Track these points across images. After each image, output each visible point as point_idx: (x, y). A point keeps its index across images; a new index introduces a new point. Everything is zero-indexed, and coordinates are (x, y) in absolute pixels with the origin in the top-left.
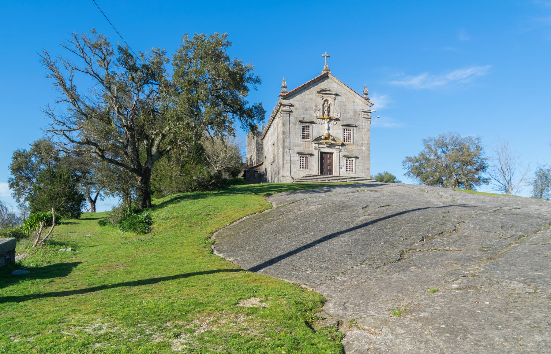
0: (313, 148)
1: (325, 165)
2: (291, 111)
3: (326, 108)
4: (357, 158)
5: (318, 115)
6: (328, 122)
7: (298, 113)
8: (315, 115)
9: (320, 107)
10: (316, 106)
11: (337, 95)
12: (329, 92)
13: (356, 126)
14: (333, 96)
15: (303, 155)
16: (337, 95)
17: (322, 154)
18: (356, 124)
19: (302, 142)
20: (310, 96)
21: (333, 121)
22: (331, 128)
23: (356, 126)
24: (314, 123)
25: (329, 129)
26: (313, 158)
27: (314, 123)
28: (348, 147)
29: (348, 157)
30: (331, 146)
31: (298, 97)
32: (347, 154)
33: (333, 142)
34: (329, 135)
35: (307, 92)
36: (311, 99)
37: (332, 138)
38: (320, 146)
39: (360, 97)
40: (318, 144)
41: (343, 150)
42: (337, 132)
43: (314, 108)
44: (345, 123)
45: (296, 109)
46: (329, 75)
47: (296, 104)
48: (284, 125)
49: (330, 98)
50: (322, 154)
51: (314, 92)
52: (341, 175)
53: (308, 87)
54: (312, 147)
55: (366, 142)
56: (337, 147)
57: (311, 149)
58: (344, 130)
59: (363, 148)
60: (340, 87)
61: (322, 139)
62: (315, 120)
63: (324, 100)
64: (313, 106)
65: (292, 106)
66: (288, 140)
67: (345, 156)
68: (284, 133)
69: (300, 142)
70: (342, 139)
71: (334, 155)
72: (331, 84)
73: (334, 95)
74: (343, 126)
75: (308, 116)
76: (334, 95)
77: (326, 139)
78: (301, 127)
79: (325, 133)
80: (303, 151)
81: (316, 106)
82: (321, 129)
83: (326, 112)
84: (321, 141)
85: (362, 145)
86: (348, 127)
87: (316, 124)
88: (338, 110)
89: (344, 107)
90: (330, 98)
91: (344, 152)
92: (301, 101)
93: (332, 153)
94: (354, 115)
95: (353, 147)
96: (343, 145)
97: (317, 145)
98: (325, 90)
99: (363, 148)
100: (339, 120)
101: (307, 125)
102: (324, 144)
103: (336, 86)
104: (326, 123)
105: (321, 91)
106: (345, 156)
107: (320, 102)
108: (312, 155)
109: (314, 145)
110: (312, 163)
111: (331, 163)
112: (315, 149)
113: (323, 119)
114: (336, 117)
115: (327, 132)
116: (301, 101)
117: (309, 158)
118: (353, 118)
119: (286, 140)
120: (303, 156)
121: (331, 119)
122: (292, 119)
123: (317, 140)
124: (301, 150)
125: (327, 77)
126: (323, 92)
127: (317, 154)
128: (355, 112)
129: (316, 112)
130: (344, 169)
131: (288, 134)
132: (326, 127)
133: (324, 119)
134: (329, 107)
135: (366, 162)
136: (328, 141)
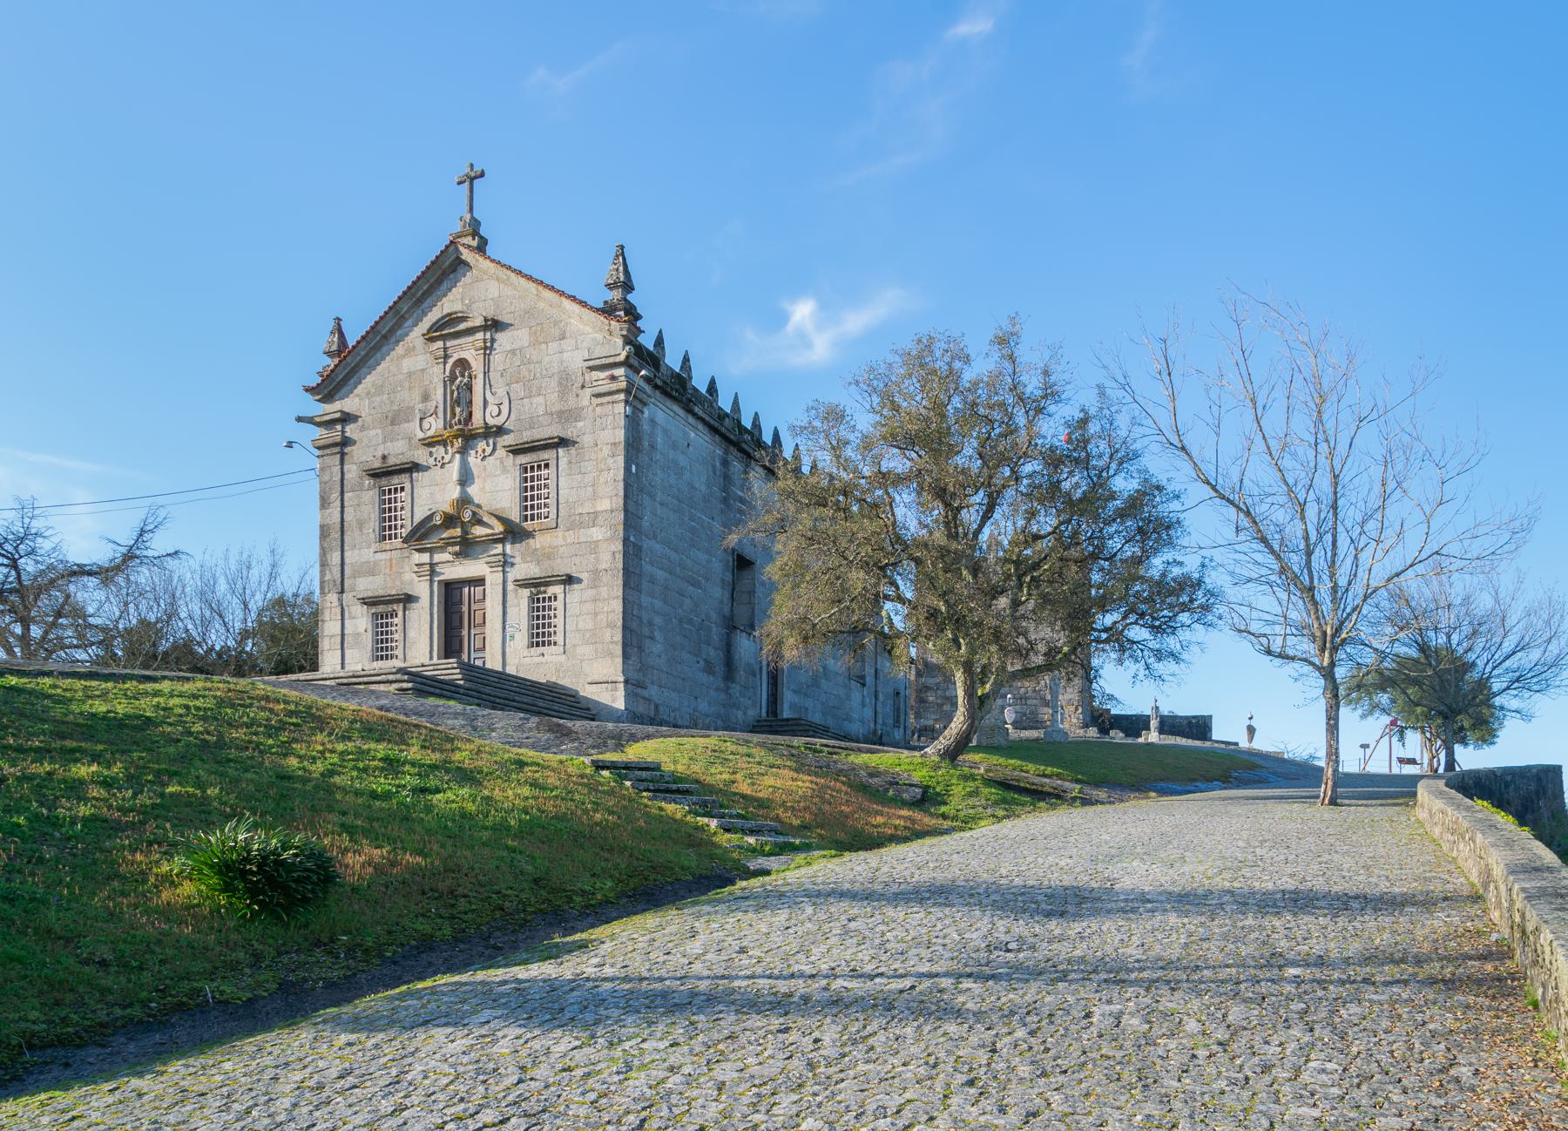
0: (408, 572)
4: (569, 580)
6: (463, 451)
7: (369, 446)
8: (421, 435)
10: (426, 398)
11: (494, 325)
12: (462, 326)
13: (563, 442)
14: (480, 335)
16: (494, 325)
18: (569, 433)
20: (408, 364)
21: (481, 445)
22: (475, 471)
23: (563, 442)
25: (465, 479)
29: (536, 585)
30: (467, 547)
34: (465, 501)
36: (410, 374)
38: (438, 557)
40: (431, 551)
41: (517, 560)
42: (496, 485)
45: (363, 428)
48: (324, 503)
50: (451, 594)
56: (499, 548)
60: (508, 291)
62: (421, 455)
63: (451, 361)
64: (412, 398)
66: (335, 558)
67: (523, 584)
68: (324, 532)
71: (488, 582)
72: (476, 293)
73: (485, 328)
74: (516, 451)
77: (450, 520)
78: (374, 493)
80: (381, 592)
87: (427, 468)
90: (467, 349)
91: (524, 568)
92: (380, 389)
96: (514, 533)
97: (425, 558)
98: (451, 320)
99: (597, 533)
100: (500, 431)
101: (396, 480)
106: (523, 584)
108: (408, 599)
110: (411, 634)
116: (380, 389)
120: (381, 608)
122: (352, 471)
123: (421, 535)
128: (565, 381)
129: (426, 425)
130: (520, 639)
134: (470, 388)
136: (458, 532)
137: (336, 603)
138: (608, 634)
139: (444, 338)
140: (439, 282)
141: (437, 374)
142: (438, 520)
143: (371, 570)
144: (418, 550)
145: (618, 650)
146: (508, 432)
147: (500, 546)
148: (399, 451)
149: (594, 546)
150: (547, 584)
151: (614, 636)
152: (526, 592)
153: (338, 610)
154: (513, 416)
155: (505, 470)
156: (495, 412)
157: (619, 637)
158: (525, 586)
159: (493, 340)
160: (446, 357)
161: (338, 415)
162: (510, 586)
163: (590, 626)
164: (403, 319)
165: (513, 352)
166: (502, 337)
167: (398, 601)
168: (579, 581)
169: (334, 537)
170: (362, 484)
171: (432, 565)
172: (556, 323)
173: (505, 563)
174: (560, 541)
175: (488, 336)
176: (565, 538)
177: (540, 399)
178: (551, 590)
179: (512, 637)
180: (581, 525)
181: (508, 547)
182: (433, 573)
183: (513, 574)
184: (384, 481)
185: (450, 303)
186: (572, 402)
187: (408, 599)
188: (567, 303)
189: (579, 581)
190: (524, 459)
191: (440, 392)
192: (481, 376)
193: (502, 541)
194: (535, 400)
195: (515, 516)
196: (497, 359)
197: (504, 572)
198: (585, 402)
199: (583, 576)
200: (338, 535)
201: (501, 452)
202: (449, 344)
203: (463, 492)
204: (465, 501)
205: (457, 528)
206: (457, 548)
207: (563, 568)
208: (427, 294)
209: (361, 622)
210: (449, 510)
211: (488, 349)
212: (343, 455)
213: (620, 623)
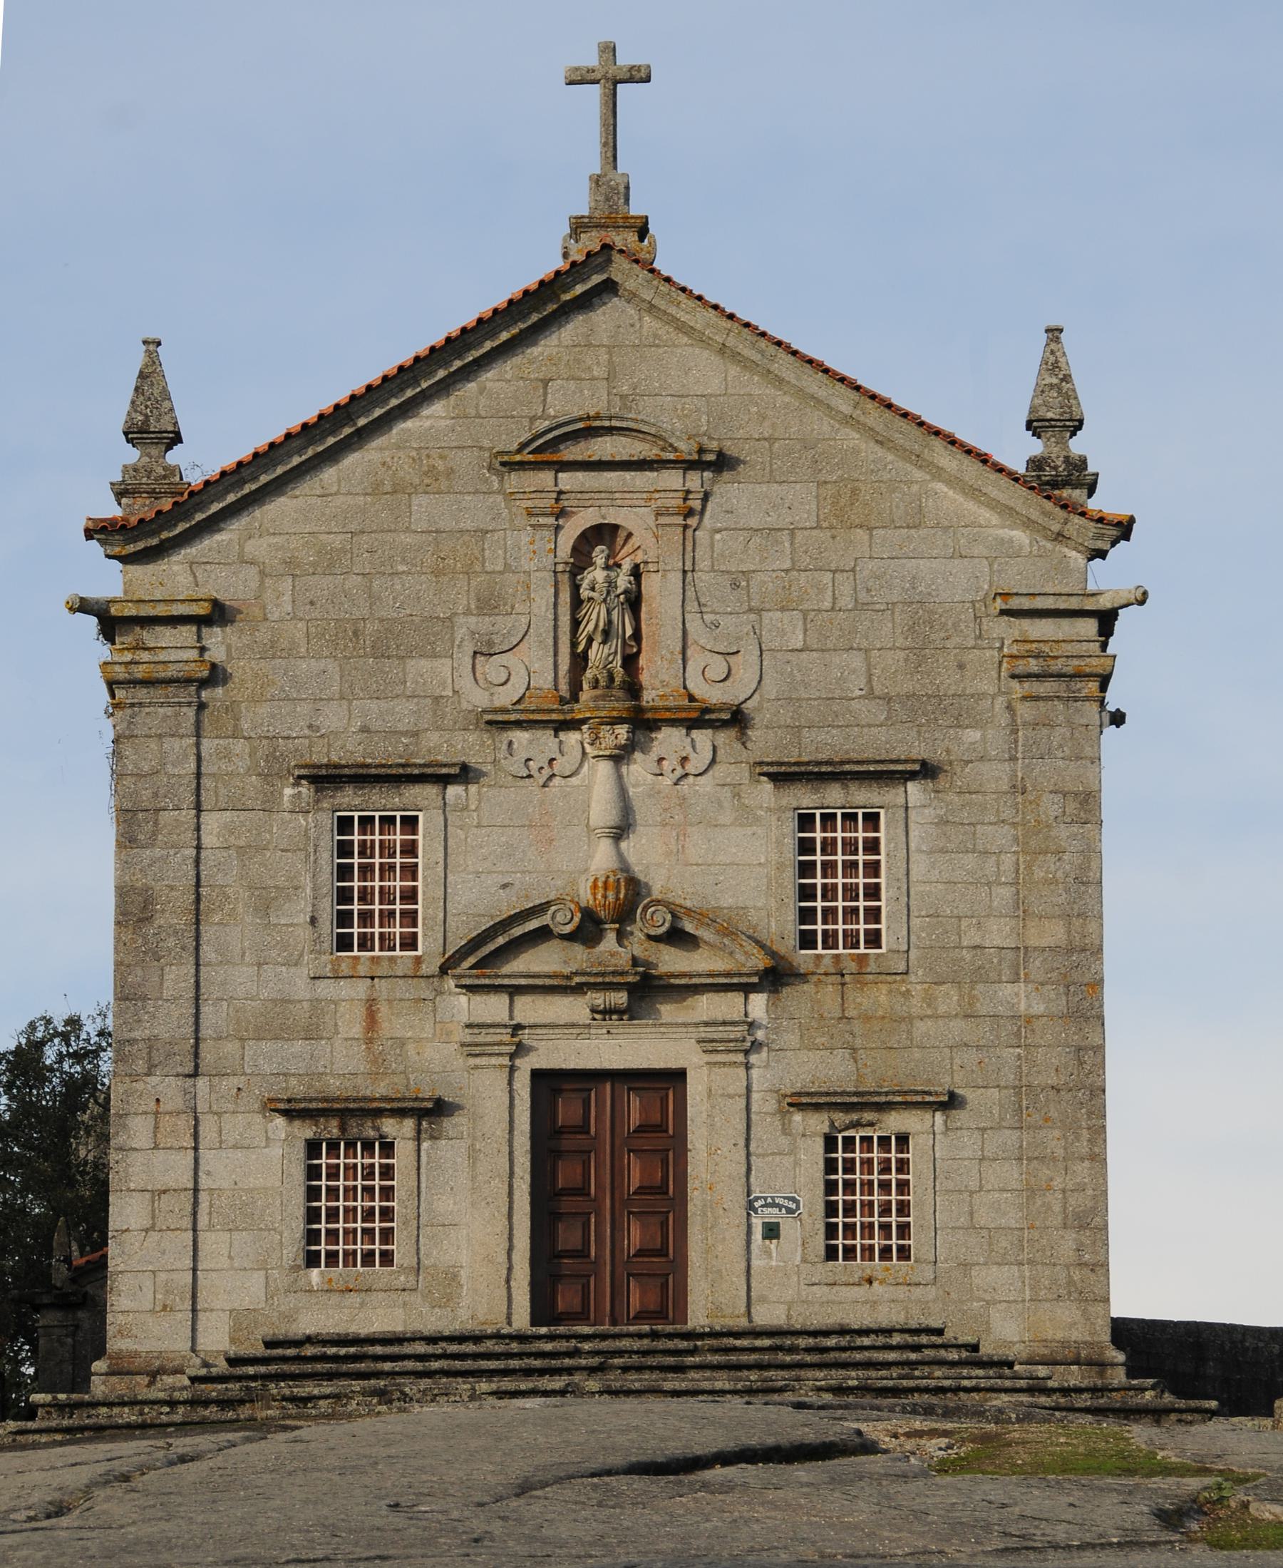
2: (216, 676)
5: (506, 697)
10: (488, 604)
13: (927, 771)
14: (672, 479)
17: (557, 1094)
19: (326, 989)
24: (465, 774)
33: (671, 961)
38: (530, 1009)
42: (722, 850)
45: (272, 650)
49: (634, 505)
52: (766, 1316)
55: (1054, 933)
58: (805, 821)
66: (177, 978)
69: (299, 986)
70: (780, 925)
74: (783, 777)
75: (403, 713)
79: (580, 867)
94: (919, 655)
97: (494, 1008)
100: (737, 719)
102: (579, 989)
104: (605, 768)
108: (432, 1112)
109: (463, 1006)
110: (443, 1204)
112: (473, 1050)
115: (604, 849)
117: (404, 1151)
122: (230, 758)
128: (923, 627)
129: (491, 669)
130: (802, 1233)
131: (172, 916)
132: (602, 811)
133: (574, 725)
134: (634, 602)
135: (1053, 1140)
141: (533, 556)
142: (564, 921)
144: (472, 989)
147: (737, 998)
152: (819, 1123)
153: (185, 1123)
155: (746, 816)
158: (817, 1107)
159: (706, 497)
160: (561, 513)
161: (202, 609)
163: (1012, 1219)
167: (401, 1113)
170: (275, 796)
171: (518, 1027)
175: (694, 480)
176: (930, 1000)
177: (857, 661)
179: (772, 1231)
184: (351, 800)
187: (432, 1112)
190: (806, 797)
193: (747, 989)
197: (748, 1067)
200: (182, 922)
201: (733, 770)
202: (567, 480)
203: (620, 856)
205: (625, 939)
206: (621, 998)
209: (262, 1164)
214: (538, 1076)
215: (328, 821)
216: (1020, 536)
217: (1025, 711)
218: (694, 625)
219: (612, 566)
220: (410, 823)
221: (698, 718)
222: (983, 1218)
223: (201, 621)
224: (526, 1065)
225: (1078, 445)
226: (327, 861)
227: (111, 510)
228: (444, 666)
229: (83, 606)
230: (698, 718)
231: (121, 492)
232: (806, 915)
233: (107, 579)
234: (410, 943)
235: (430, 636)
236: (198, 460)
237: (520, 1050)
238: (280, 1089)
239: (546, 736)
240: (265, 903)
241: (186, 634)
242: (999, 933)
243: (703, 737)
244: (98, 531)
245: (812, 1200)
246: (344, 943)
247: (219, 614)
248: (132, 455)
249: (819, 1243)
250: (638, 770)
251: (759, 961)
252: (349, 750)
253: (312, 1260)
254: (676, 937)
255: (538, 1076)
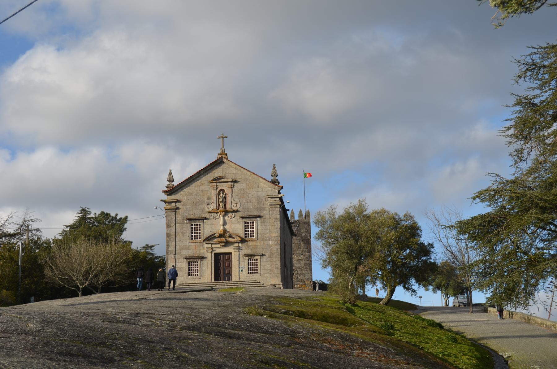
0: (204, 250)
1: (222, 268)
2: (178, 208)
3: (221, 200)
4: (262, 255)
5: (211, 209)
6: (224, 216)
7: (186, 210)
8: (207, 210)
9: (214, 198)
10: (209, 198)
11: (235, 181)
13: (260, 217)
14: (230, 183)
15: (192, 260)
16: (235, 181)
17: (217, 256)
19: (190, 244)
20: (201, 188)
21: (230, 214)
22: (227, 222)
23: (260, 217)
24: (206, 219)
25: (225, 224)
26: (205, 262)
27: (206, 219)
28: (250, 244)
29: (250, 256)
30: (227, 244)
31: (186, 190)
32: (249, 252)
34: (225, 231)
35: (198, 183)
36: (203, 191)
37: (228, 235)
38: (214, 246)
39: (264, 181)
40: (212, 244)
41: (243, 248)
42: (236, 226)
43: (206, 201)
44: (246, 214)
45: (184, 205)
46: (225, 160)
47: (184, 199)
48: (168, 226)
49: (226, 187)
50: (217, 256)
51: (206, 183)
53: (198, 177)
54: (204, 249)
56: (236, 245)
57: (202, 251)
58: (245, 223)
59: (271, 242)
61: (215, 237)
62: (207, 216)
63: (218, 190)
65: (178, 201)
66: (173, 243)
68: (168, 235)
70: (243, 235)
71: (233, 254)
73: (231, 182)
74: (243, 218)
76: (231, 182)
77: (221, 236)
78: (189, 226)
80: (191, 255)
81: (209, 198)
82: (215, 225)
83: (221, 204)
84: (215, 240)
85: (270, 238)
86: (249, 219)
88: (237, 200)
89: (245, 195)
93: (231, 253)
95: (258, 243)
96: (243, 241)
97: (210, 246)
98: (220, 178)
99: (271, 242)
100: (237, 211)
101: (198, 222)
102: (219, 243)
103: (234, 171)
105: (214, 180)
107: (213, 193)
108: (203, 258)
109: (206, 246)
111: (230, 266)
112: (207, 251)
113: (217, 213)
114: (234, 209)
117: (199, 262)
118: (257, 207)
119: (170, 244)
120: (191, 260)
121: (226, 212)
122: (179, 218)
123: (209, 239)
124: (190, 253)
125: (224, 163)
126: (217, 180)
127: (210, 257)
128: (259, 199)
129: (209, 206)
130: (245, 271)
131: (173, 236)
134: (225, 198)
137: (173, 257)
138: (276, 271)
139: (216, 183)
140: (214, 166)
142: (217, 235)
143: (188, 249)
145: (280, 275)
146: (239, 211)
148: (197, 213)
149: (270, 246)
150: (255, 256)
151: (278, 272)
152: (247, 258)
153: (174, 260)
154: (241, 208)
155: (238, 222)
156: (235, 205)
157: (279, 272)
160: (217, 188)
162: (241, 256)
164: (201, 175)
165: (241, 189)
166: (236, 184)
168: (265, 255)
169: (171, 237)
171: (212, 248)
172: (255, 183)
173: (239, 249)
174: (258, 244)
177: (251, 204)
178: (256, 258)
179: (242, 271)
180: (265, 240)
181: (240, 244)
182: (212, 251)
183: (242, 253)
185: (217, 172)
186: (262, 205)
187: (203, 258)
188: (260, 179)
189: (265, 255)
191: (215, 198)
192: (230, 195)
193: (238, 243)
194: (249, 204)
195: (243, 235)
196: (235, 190)
198: (266, 206)
199: (267, 254)
202: (218, 184)
204: (225, 231)
205: (224, 237)
207: (261, 252)
208: (210, 169)
210: (221, 233)
211: (232, 187)
212: (176, 212)
213: (280, 268)
214: (215, 254)
215: (190, 225)
216: (270, 189)
217: (271, 209)
218: (232, 201)
219: (223, 194)
220: (200, 225)
221: (233, 211)
222: (266, 268)
223: (176, 202)
224: (213, 252)
225: (277, 178)
226: (190, 229)
227: (166, 189)
228: (203, 206)
229: (162, 201)
230: (233, 211)
231: (167, 187)
232: (246, 234)
233: (165, 197)
234: (200, 238)
235: (202, 203)
236: (175, 183)
237: (212, 251)
238: (185, 256)
239: (215, 214)
240: (183, 234)
241: (174, 204)
242: (268, 235)
243: (234, 214)
244: (164, 192)
245: (246, 267)
246: (192, 239)
247: (178, 201)
248: (168, 183)
249: (247, 272)
250: (226, 218)
251: (240, 239)
252: (192, 217)
253: (189, 275)
254: (230, 237)
255: (215, 254)
